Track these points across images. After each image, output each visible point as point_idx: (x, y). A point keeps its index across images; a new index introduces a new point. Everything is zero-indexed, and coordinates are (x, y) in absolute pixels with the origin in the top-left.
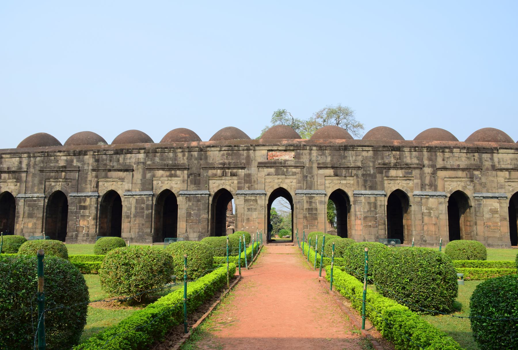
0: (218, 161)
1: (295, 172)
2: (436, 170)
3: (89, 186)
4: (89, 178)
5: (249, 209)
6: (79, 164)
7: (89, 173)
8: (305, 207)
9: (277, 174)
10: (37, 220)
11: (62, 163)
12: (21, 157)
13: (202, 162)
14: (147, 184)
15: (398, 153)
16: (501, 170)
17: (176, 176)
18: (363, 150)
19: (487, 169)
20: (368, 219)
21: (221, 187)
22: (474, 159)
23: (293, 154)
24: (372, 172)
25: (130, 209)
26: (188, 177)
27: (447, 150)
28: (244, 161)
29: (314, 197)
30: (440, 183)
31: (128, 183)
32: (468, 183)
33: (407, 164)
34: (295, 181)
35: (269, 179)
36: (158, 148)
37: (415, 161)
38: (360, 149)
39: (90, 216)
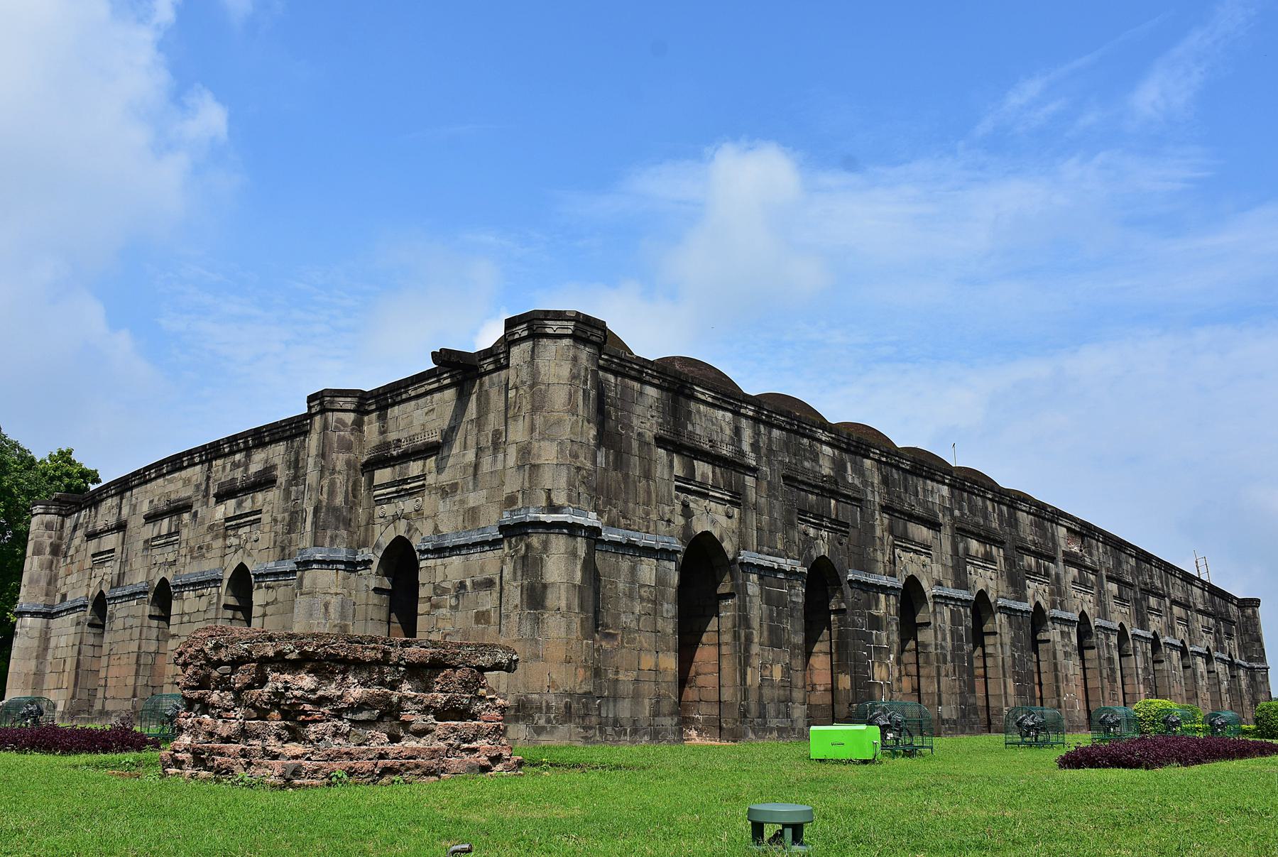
3: (879, 555)
4: (878, 532)
6: (857, 482)
7: (877, 516)
10: (792, 656)
11: (826, 470)
12: (736, 413)
39: (889, 651)
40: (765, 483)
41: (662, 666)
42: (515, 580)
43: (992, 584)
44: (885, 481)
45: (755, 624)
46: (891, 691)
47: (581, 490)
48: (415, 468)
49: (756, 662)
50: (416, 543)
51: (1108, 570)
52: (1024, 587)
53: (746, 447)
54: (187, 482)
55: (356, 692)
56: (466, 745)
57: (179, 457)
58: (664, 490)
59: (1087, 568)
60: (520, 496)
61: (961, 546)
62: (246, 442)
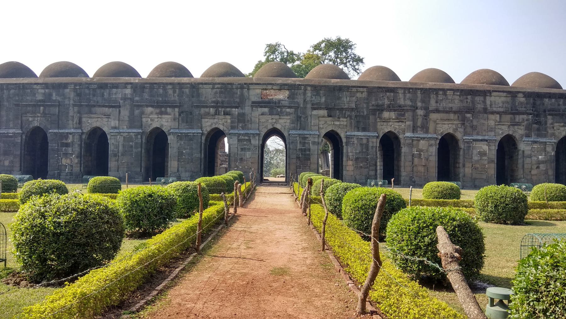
0: (211, 99)
1: (289, 112)
2: (428, 111)
3: (70, 122)
4: (71, 113)
5: (242, 149)
6: (59, 98)
7: (71, 108)
8: (298, 148)
9: (271, 114)
11: (39, 97)
13: (194, 99)
14: (135, 121)
15: (392, 94)
16: (493, 113)
17: (166, 113)
18: (357, 92)
19: (479, 112)
20: (360, 159)
21: (214, 126)
22: (467, 102)
23: (287, 93)
24: (365, 113)
25: (117, 147)
26: (180, 115)
27: (441, 93)
28: (238, 100)
29: (307, 137)
30: (431, 126)
31: (114, 120)
32: (459, 126)
33: (400, 106)
34: (289, 121)
35: (263, 119)
36: (146, 83)
37: (409, 103)
38: (354, 90)
39: (72, 154)
61: (137, 112)
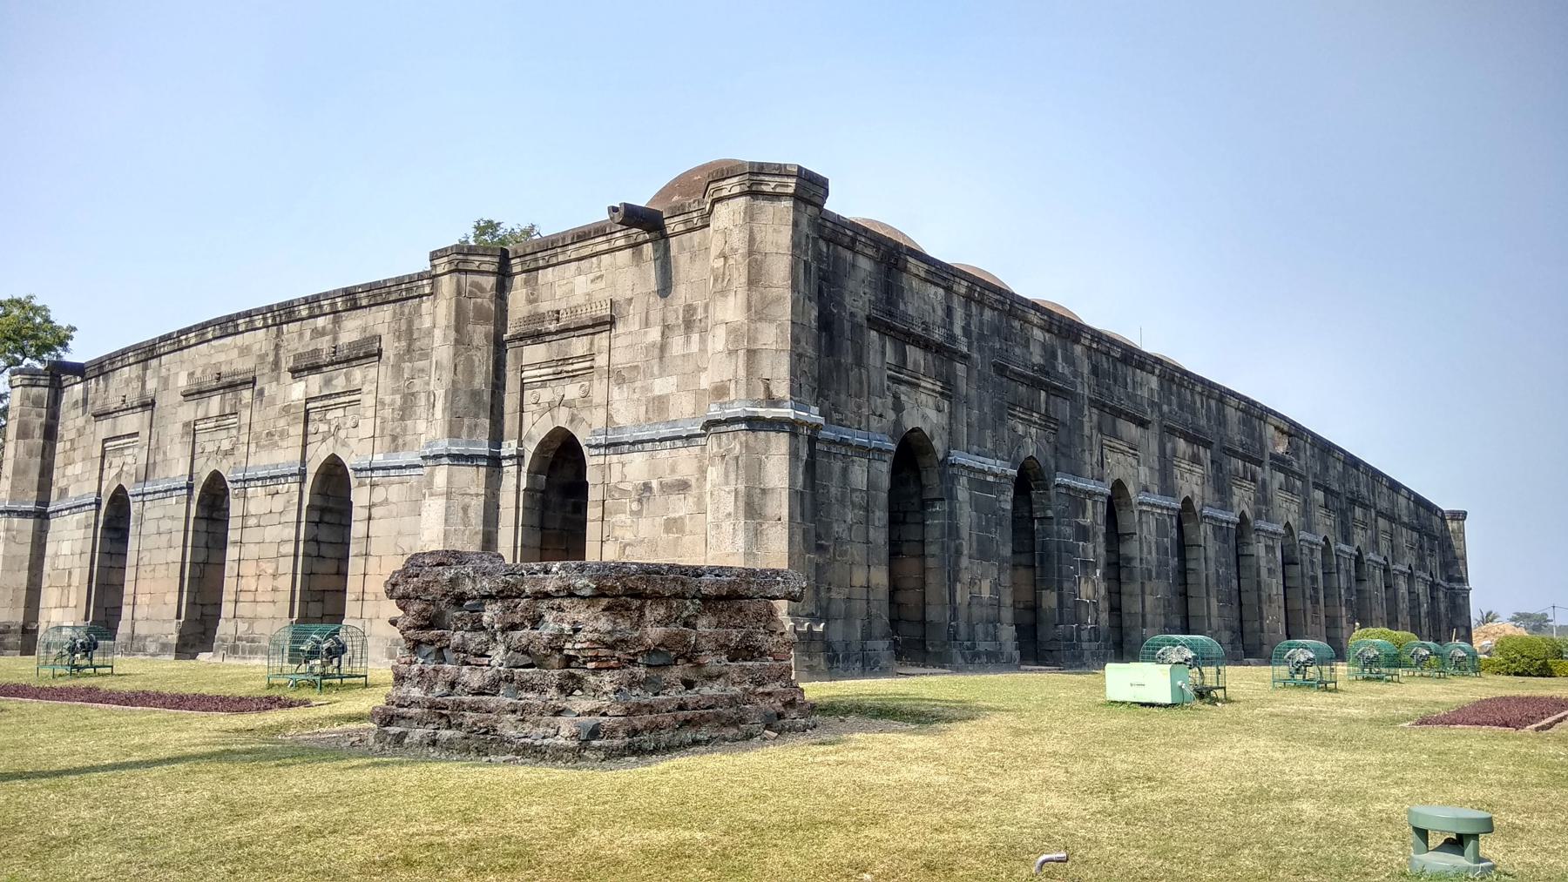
4: (1087, 431)
6: (1066, 371)
11: (1037, 359)
12: (948, 290)
39: (1095, 565)
40: (975, 373)
41: (873, 582)
42: (727, 483)
43: (1197, 490)
44: (1095, 371)
45: (965, 533)
46: (1097, 610)
47: (803, 380)
48: (579, 346)
49: (966, 577)
50: (582, 437)
51: (1315, 476)
52: (1232, 494)
53: (958, 331)
54: (244, 351)
55: (654, 633)
56: (760, 690)
57: (231, 319)
58: (875, 380)
59: (1293, 472)
60: (732, 386)
61: (1169, 446)
62: (333, 305)
